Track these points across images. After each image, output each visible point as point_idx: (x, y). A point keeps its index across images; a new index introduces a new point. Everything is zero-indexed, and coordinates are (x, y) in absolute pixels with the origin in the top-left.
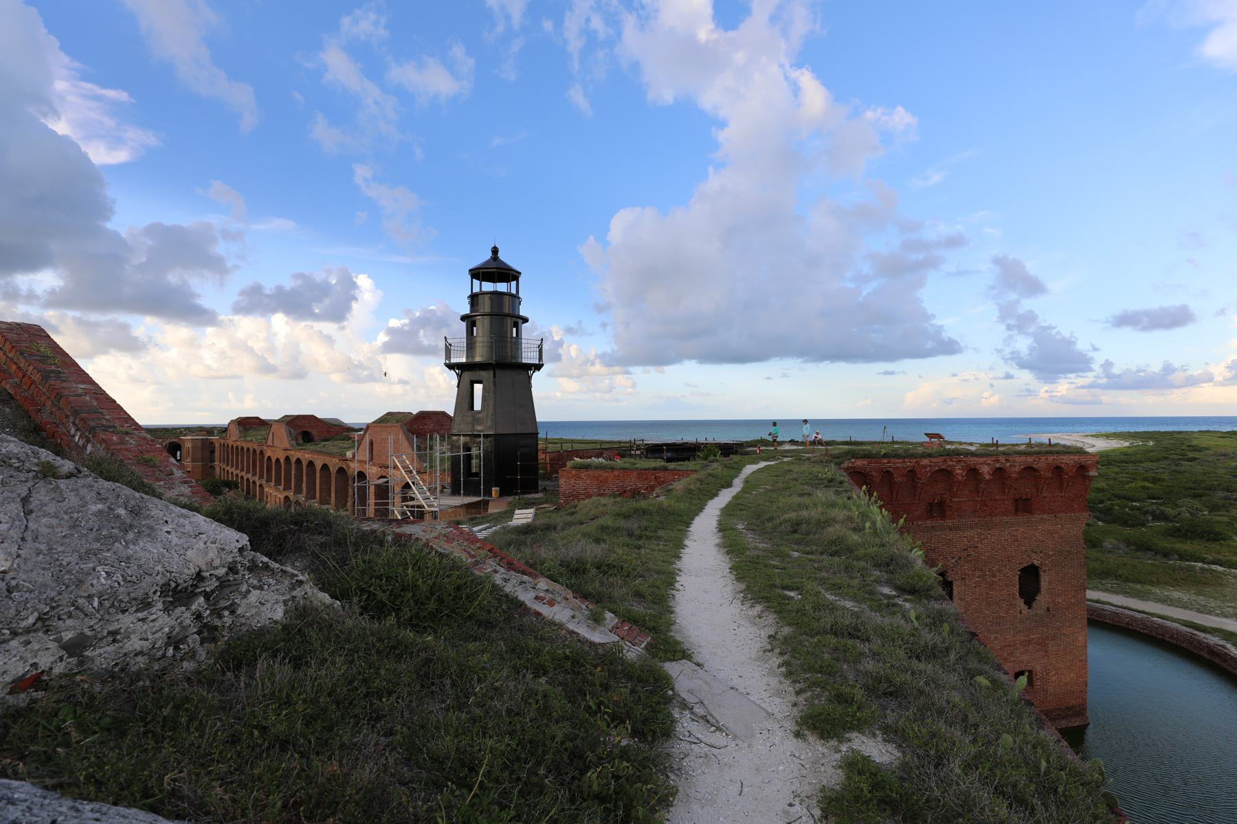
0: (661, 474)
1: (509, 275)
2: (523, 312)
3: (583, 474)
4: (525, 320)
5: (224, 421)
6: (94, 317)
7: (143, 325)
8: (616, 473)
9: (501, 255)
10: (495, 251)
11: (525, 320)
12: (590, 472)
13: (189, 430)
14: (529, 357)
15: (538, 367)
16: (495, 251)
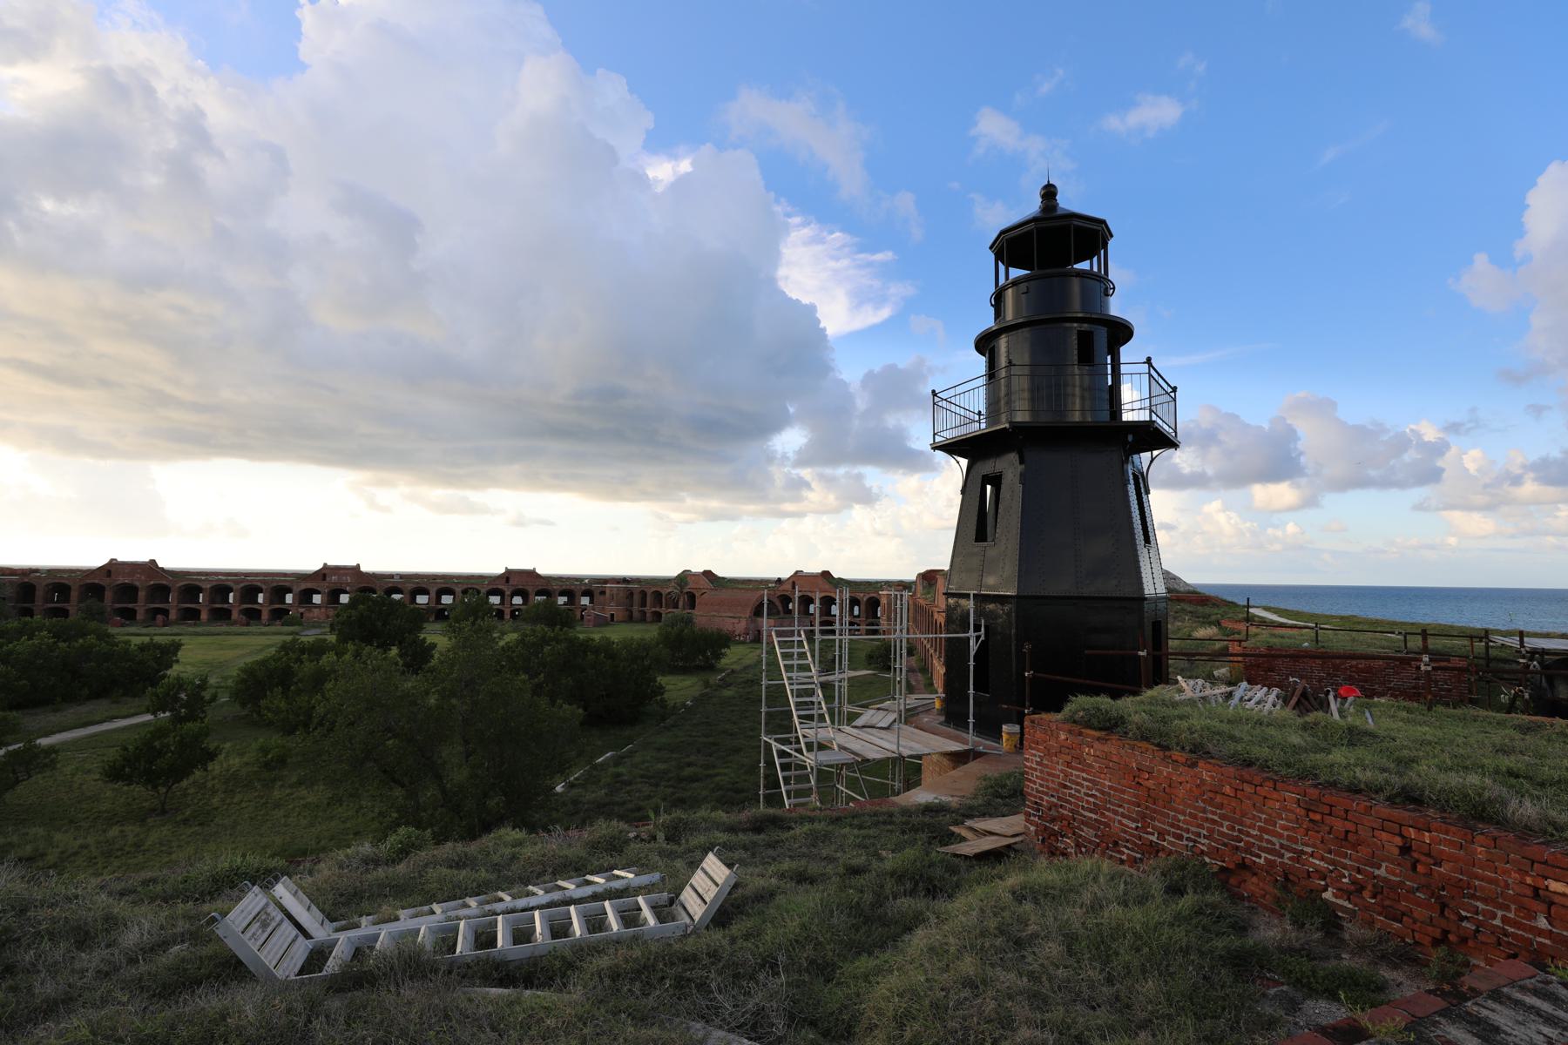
0: (1438, 839)
1: (1090, 236)
2: (1116, 307)
3: (1093, 749)
4: (1121, 332)
5: (912, 577)
6: (828, 471)
7: (873, 476)
8: (1205, 773)
9: (1068, 201)
10: (1049, 193)
11: (1121, 332)
12: (1111, 747)
13: (888, 584)
14: (1133, 408)
15: (1153, 437)
16: (1049, 193)
